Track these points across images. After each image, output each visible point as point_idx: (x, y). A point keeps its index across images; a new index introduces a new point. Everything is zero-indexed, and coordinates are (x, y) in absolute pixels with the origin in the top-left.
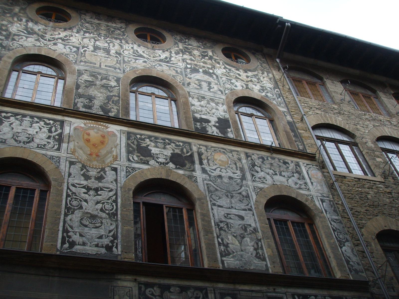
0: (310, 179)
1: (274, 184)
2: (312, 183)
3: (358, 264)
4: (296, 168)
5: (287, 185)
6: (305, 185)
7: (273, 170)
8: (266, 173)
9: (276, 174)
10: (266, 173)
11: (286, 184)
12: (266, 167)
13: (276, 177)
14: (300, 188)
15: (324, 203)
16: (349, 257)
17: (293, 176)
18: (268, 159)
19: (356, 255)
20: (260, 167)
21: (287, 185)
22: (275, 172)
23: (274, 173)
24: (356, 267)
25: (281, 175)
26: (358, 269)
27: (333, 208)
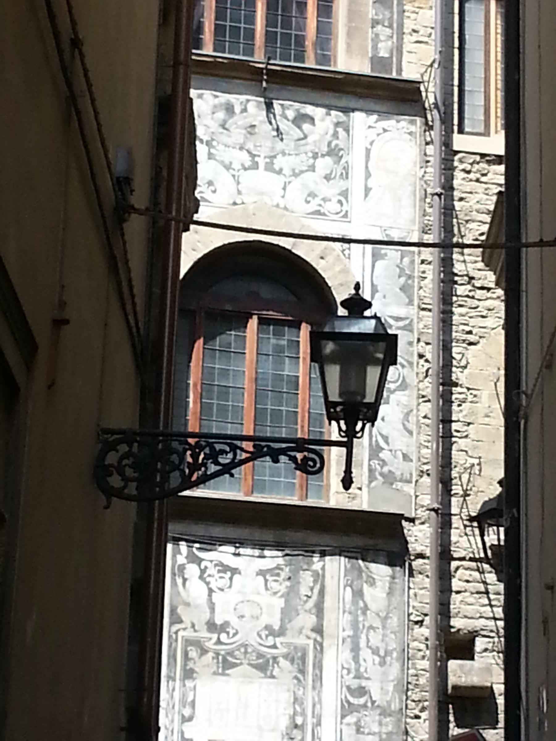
0: (368, 175)
1: (235, 204)
2: (367, 190)
3: (406, 457)
4: (335, 135)
5: (277, 206)
6: (340, 202)
7: (249, 152)
8: (222, 163)
9: (255, 166)
10: (222, 163)
11: (277, 199)
12: (229, 141)
13: (248, 179)
14: (318, 212)
15: (379, 264)
16: (386, 439)
17: (312, 168)
18: (245, 110)
19: (411, 433)
20: (208, 144)
21: (277, 206)
22: (253, 156)
23: (248, 164)
24: (397, 466)
25: (269, 167)
26: (398, 473)
27: (403, 280)
